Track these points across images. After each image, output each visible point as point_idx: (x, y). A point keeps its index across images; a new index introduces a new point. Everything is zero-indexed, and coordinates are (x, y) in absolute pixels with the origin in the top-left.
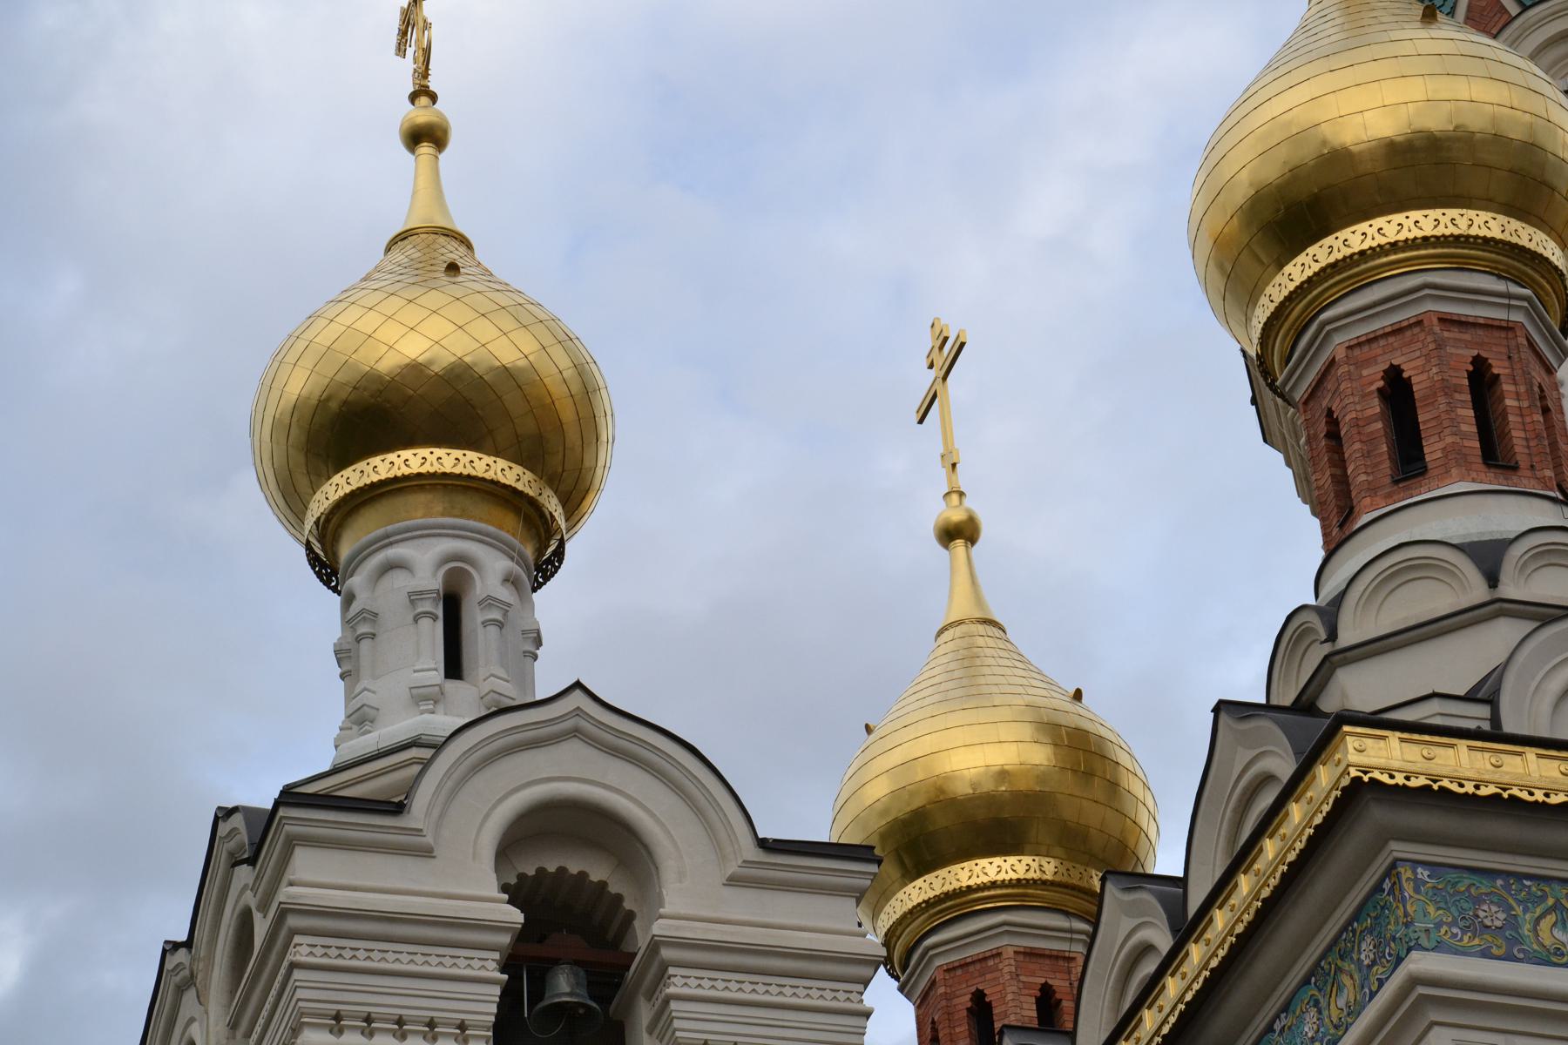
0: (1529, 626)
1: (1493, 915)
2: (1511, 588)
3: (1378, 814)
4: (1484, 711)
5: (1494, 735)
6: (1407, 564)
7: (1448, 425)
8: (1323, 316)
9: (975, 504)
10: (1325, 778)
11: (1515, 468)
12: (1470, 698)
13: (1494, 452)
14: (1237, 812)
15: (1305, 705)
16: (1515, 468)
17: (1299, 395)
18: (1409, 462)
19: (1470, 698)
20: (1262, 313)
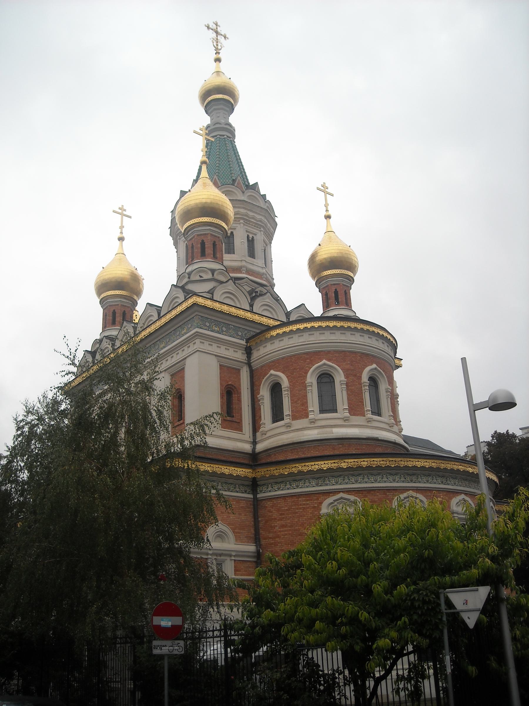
0: (219, 284)
1: (208, 324)
2: (216, 276)
3: (196, 308)
4: (211, 295)
5: (212, 299)
6: (201, 270)
7: (209, 250)
8: (195, 229)
9: (124, 235)
10: (190, 301)
11: (217, 258)
12: (208, 292)
13: (215, 257)
14: (170, 299)
15: (183, 288)
16: (217, 258)
17: (188, 239)
18: (203, 254)
19: (208, 292)
20: (185, 226)
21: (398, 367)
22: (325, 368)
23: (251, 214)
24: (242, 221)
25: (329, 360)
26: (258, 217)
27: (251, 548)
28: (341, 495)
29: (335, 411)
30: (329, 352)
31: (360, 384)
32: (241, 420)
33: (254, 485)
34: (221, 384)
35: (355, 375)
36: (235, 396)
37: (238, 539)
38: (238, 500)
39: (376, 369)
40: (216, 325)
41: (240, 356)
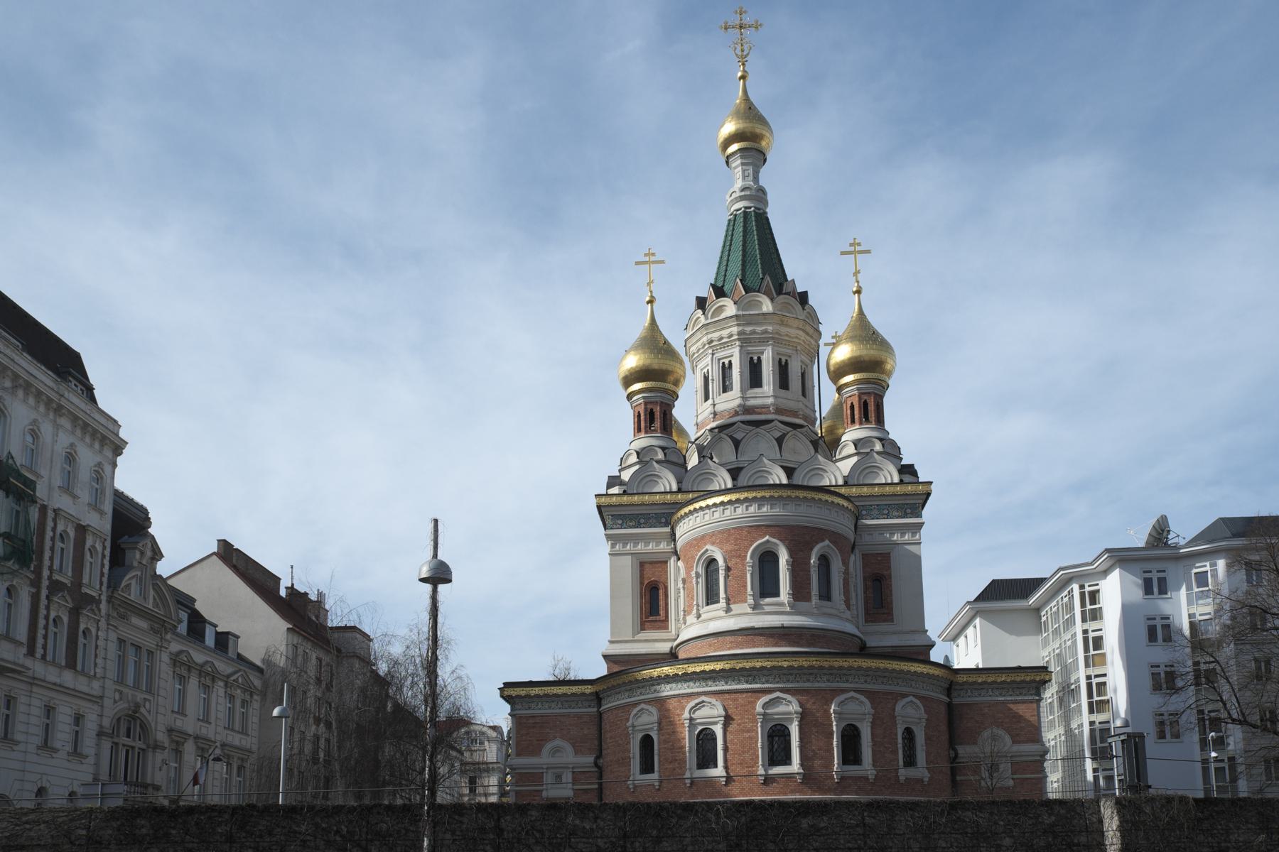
21: (928, 495)
22: (709, 554)
23: (748, 329)
24: (738, 343)
25: (713, 544)
26: (759, 329)
27: (591, 759)
28: (643, 706)
29: (718, 602)
30: (713, 534)
31: (744, 565)
32: (667, 616)
33: (598, 698)
34: (642, 583)
35: (739, 556)
36: (661, 592)
37: (577, 752)
38: (579, 716)
39: (768, 541)
40: (631, 520)
41: (664, 546)
